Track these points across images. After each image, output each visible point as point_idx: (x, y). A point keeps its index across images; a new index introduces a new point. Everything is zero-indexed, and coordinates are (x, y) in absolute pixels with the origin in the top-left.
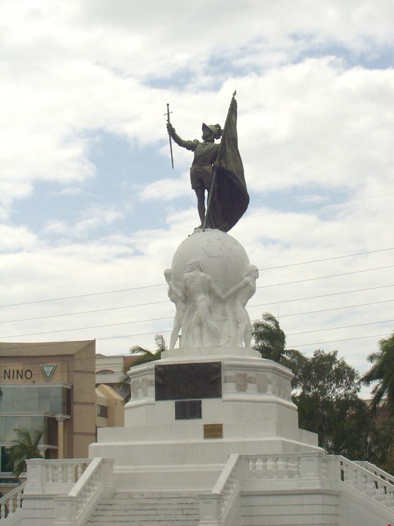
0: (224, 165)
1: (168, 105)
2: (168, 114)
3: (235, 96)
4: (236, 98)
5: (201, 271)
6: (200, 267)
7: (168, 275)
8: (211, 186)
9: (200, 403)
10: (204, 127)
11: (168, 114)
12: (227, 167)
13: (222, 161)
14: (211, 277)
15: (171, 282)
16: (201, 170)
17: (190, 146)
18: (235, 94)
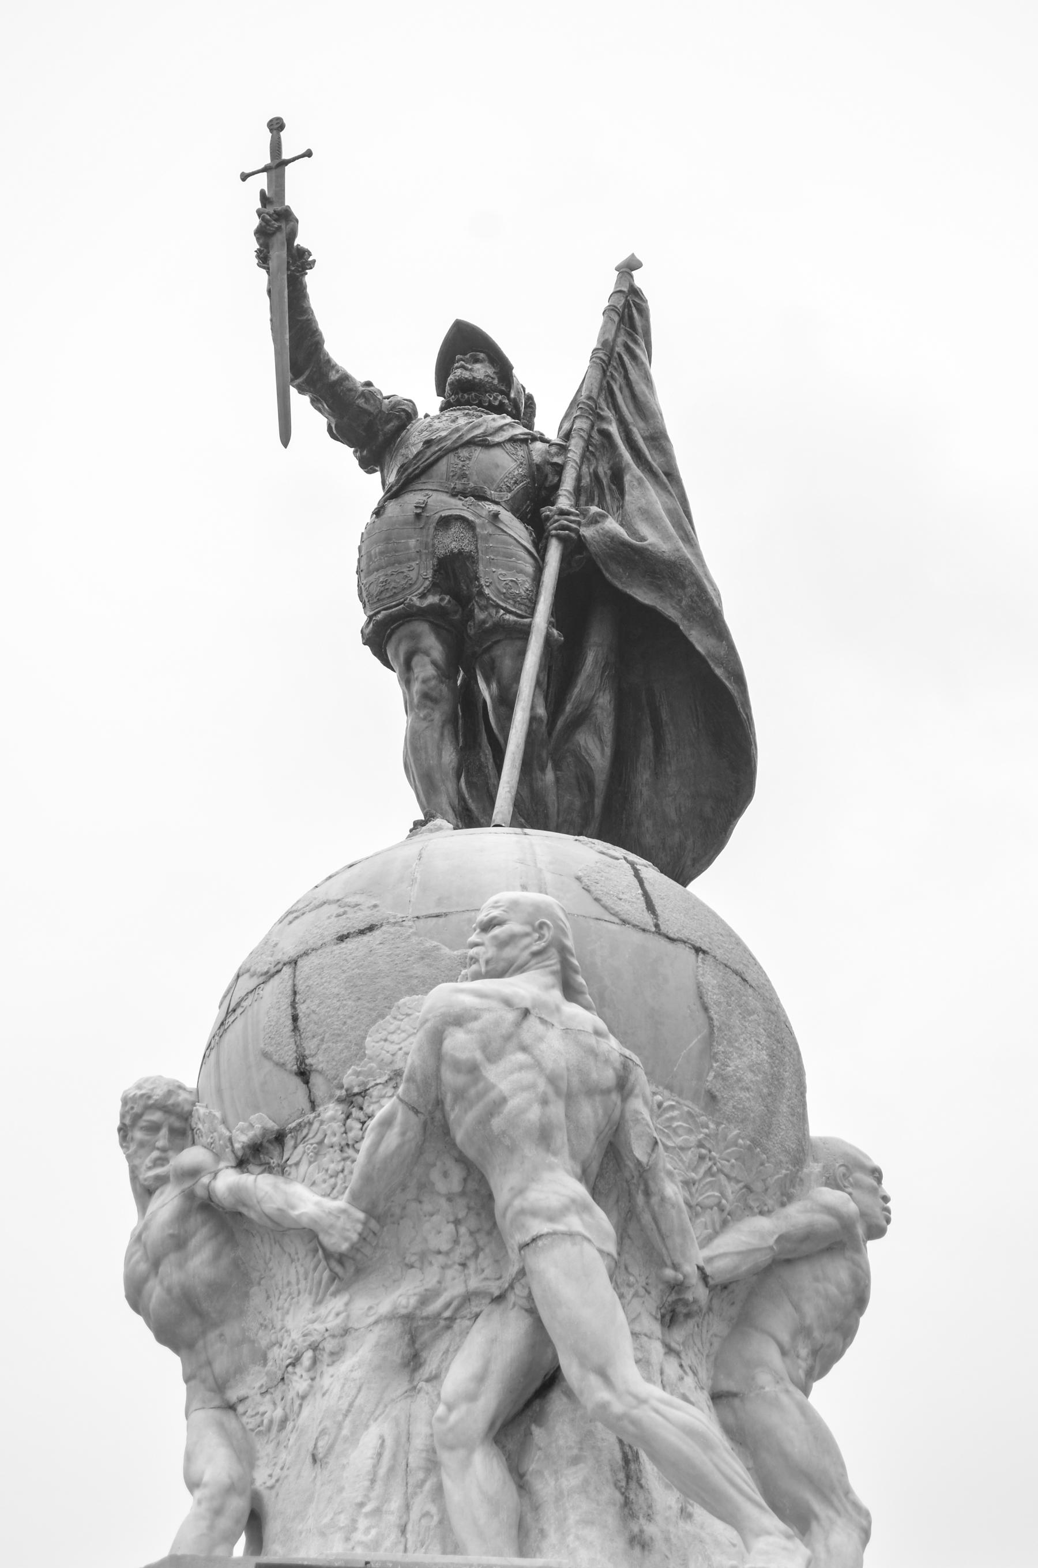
1: (276, 126)
2: (277, 167)
4: (639, 278)
5: (570, 991)
6: (563, 951)
10: (465, 343)
11: (277, 167)
12: (643, 539)
13: (594, 509)
14: (628, 1053)
15: (192, 1155)
16: (471, 518)
17: (368, 425)
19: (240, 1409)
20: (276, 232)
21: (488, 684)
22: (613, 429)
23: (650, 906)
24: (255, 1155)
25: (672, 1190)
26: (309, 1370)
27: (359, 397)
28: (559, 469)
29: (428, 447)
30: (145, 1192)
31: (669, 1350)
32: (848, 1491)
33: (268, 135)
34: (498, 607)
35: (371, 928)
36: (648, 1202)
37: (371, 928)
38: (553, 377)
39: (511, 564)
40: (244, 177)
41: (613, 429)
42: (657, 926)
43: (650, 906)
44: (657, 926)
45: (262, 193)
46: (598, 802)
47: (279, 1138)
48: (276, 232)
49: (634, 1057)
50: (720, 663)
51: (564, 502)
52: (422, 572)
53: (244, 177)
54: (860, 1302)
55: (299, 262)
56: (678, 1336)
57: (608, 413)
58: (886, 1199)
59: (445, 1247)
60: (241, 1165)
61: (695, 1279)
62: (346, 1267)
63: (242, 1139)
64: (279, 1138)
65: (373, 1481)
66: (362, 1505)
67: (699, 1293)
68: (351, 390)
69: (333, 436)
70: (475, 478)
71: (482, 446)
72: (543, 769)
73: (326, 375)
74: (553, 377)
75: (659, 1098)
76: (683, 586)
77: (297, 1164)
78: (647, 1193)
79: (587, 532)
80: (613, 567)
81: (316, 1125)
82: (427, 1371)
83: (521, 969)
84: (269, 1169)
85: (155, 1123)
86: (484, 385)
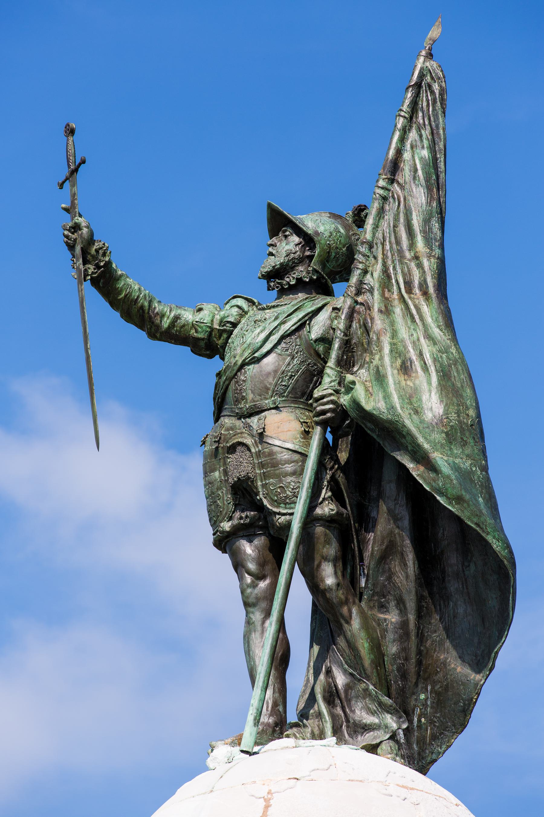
27: (191, 328)
29: (220, 378)
34: (275, 513)
39: (277, 472)
40: (61, 186)
46: (412, 617)
50: (441, 494)
52: (226, 498)
68: (184, 326)
70: (250, 396)
71: (254, 363)
72: (348, 622)
73: (158, 327)
76: (404, 437)
79: (344, 400)
80: (369, 425)
86: (287, 265)
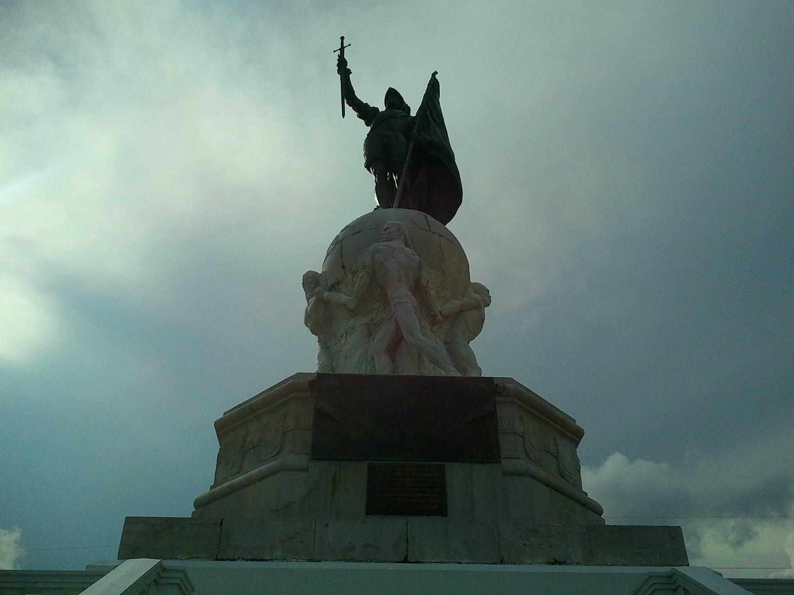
0: (426, 136)
1: (342, 38)
2: (342, 49)
3: (436, 75)
5: (407, 245)
6: (405, 234)
7: (311, 281)
8: (406, 157)
9: (442, 470)
11: (342, 49)
18: (436, 73)
19: (330, 348)
20: (342, 65)
21: (395, 176)
22: (428, 113)
23: (428, 225)
24: (333, 288)
25: (432, 293)
26: (345, 338)
28: (414, 123)
30: (308, 300)
31: (432, 331)
32: (477, 364)
33: (340, 40)
35: (360, 232)
36: (426, 296)
37: (360, 232)
38: (414, 102)
40: (335, 51)
41: (428, 113)
42: (430, 229)
43: (428, 225)
44: (430, 229)
45: (339, 55)
47: (338, 283)
48: (342, 65)
49: (423, 261)
51: (415, 131)
53: (335, 51)
54: (483, 320)
55: (349, 72)
56: (435, 328)
57: (427, 110)
58: (490, 297)
59: (377, 307)
60: (330, 290)
61: (439, 314)
62: (354, 313)
63: (329, 284)
64: (338, 283)
65: (358, 363)
66: (356, 368)
67: (440, 317)
69: (358, 117)
74: (414, 102)
75: (430, 271)
77: (342, 289)
78: (426, 293)
81: (346, 279)
82: (372, 337)
83: (393, 240)
84: (336, 291)
85: (311, 281)
